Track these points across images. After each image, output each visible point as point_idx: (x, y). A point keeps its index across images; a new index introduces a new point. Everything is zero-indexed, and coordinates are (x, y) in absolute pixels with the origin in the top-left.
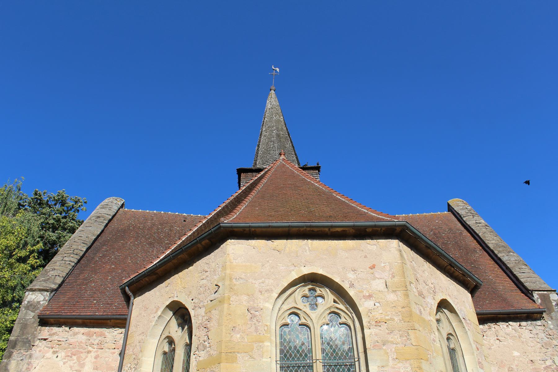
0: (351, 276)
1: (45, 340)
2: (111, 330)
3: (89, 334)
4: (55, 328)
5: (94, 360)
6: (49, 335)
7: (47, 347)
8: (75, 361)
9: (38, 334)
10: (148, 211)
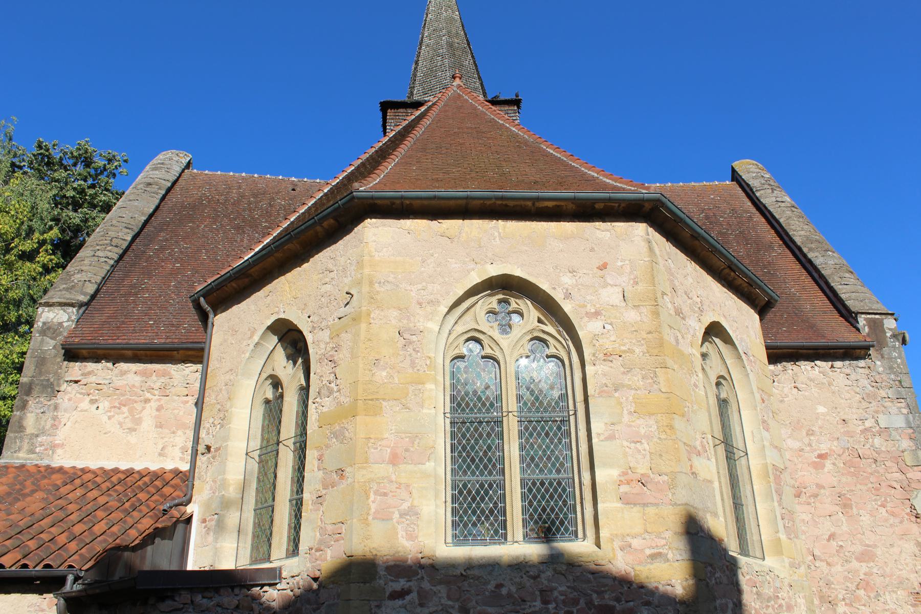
0: (567, 280)
1: (76, 382)
2: (180, 366)
3: (145, 373)
4: (90, 364)
5: (155, 413)
6: (82, 375)
7: (81, 393)
8: (127, 414)
9: (63, 372)
10: (231, 174)
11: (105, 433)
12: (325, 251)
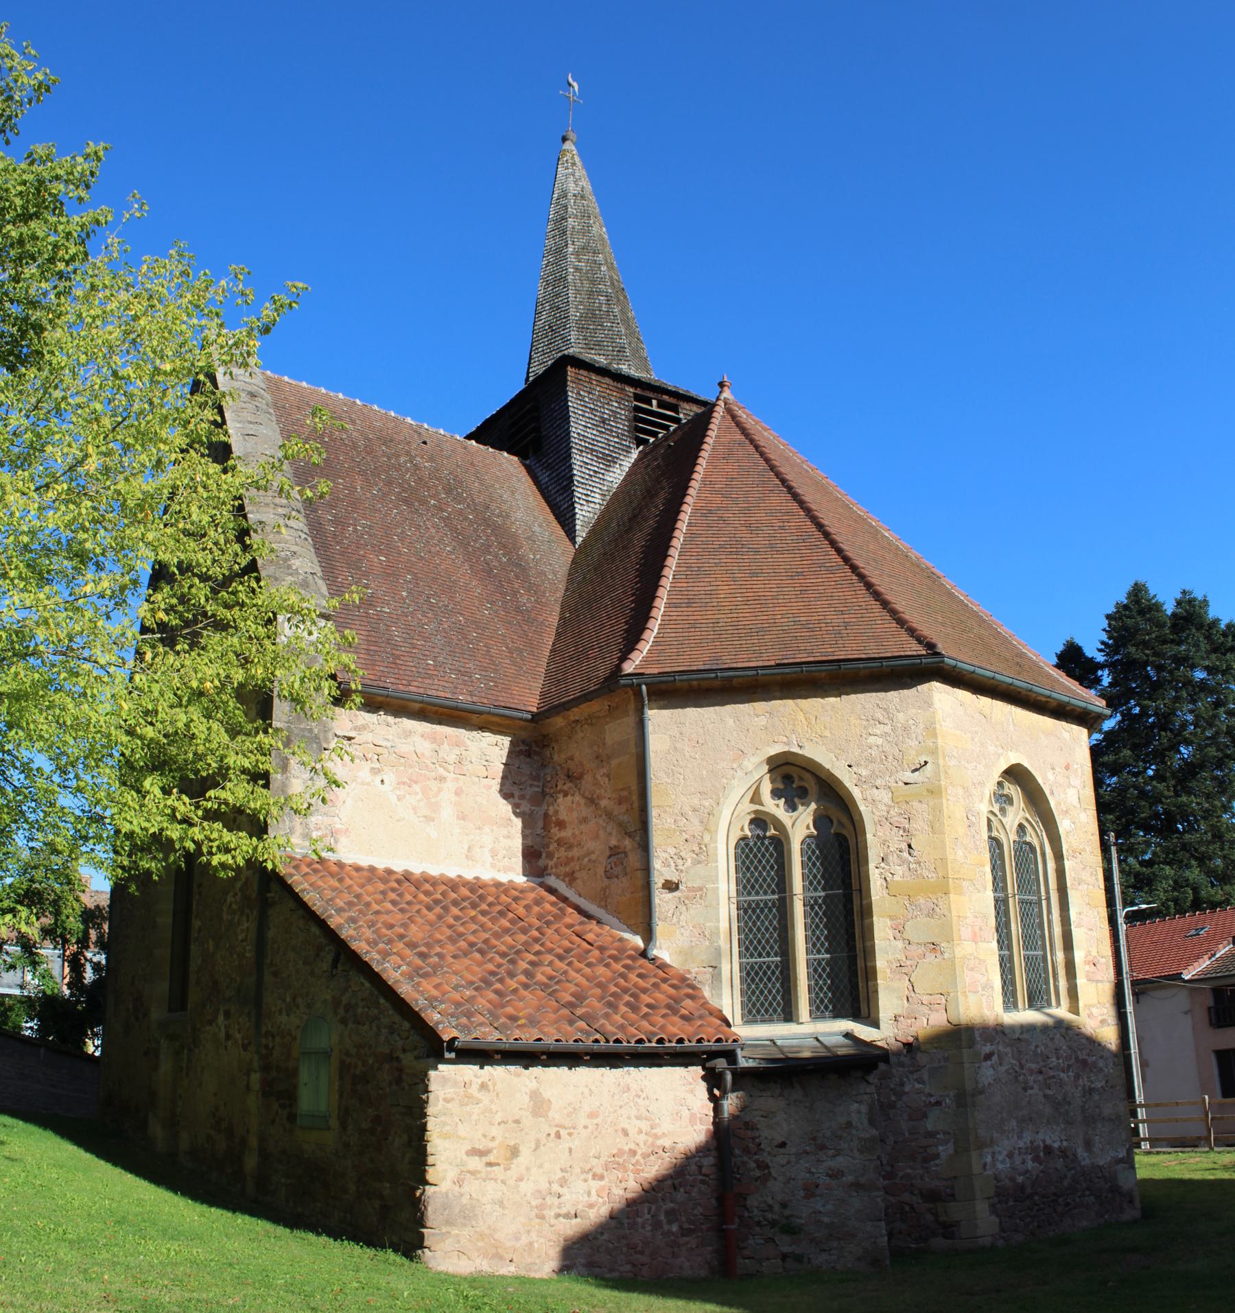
2: (476, 734)
3: (435, 738)
5: (454, 799)
6: (355, 729)
8: (419, 796)
11: (398, 821)
12: (868, 694)
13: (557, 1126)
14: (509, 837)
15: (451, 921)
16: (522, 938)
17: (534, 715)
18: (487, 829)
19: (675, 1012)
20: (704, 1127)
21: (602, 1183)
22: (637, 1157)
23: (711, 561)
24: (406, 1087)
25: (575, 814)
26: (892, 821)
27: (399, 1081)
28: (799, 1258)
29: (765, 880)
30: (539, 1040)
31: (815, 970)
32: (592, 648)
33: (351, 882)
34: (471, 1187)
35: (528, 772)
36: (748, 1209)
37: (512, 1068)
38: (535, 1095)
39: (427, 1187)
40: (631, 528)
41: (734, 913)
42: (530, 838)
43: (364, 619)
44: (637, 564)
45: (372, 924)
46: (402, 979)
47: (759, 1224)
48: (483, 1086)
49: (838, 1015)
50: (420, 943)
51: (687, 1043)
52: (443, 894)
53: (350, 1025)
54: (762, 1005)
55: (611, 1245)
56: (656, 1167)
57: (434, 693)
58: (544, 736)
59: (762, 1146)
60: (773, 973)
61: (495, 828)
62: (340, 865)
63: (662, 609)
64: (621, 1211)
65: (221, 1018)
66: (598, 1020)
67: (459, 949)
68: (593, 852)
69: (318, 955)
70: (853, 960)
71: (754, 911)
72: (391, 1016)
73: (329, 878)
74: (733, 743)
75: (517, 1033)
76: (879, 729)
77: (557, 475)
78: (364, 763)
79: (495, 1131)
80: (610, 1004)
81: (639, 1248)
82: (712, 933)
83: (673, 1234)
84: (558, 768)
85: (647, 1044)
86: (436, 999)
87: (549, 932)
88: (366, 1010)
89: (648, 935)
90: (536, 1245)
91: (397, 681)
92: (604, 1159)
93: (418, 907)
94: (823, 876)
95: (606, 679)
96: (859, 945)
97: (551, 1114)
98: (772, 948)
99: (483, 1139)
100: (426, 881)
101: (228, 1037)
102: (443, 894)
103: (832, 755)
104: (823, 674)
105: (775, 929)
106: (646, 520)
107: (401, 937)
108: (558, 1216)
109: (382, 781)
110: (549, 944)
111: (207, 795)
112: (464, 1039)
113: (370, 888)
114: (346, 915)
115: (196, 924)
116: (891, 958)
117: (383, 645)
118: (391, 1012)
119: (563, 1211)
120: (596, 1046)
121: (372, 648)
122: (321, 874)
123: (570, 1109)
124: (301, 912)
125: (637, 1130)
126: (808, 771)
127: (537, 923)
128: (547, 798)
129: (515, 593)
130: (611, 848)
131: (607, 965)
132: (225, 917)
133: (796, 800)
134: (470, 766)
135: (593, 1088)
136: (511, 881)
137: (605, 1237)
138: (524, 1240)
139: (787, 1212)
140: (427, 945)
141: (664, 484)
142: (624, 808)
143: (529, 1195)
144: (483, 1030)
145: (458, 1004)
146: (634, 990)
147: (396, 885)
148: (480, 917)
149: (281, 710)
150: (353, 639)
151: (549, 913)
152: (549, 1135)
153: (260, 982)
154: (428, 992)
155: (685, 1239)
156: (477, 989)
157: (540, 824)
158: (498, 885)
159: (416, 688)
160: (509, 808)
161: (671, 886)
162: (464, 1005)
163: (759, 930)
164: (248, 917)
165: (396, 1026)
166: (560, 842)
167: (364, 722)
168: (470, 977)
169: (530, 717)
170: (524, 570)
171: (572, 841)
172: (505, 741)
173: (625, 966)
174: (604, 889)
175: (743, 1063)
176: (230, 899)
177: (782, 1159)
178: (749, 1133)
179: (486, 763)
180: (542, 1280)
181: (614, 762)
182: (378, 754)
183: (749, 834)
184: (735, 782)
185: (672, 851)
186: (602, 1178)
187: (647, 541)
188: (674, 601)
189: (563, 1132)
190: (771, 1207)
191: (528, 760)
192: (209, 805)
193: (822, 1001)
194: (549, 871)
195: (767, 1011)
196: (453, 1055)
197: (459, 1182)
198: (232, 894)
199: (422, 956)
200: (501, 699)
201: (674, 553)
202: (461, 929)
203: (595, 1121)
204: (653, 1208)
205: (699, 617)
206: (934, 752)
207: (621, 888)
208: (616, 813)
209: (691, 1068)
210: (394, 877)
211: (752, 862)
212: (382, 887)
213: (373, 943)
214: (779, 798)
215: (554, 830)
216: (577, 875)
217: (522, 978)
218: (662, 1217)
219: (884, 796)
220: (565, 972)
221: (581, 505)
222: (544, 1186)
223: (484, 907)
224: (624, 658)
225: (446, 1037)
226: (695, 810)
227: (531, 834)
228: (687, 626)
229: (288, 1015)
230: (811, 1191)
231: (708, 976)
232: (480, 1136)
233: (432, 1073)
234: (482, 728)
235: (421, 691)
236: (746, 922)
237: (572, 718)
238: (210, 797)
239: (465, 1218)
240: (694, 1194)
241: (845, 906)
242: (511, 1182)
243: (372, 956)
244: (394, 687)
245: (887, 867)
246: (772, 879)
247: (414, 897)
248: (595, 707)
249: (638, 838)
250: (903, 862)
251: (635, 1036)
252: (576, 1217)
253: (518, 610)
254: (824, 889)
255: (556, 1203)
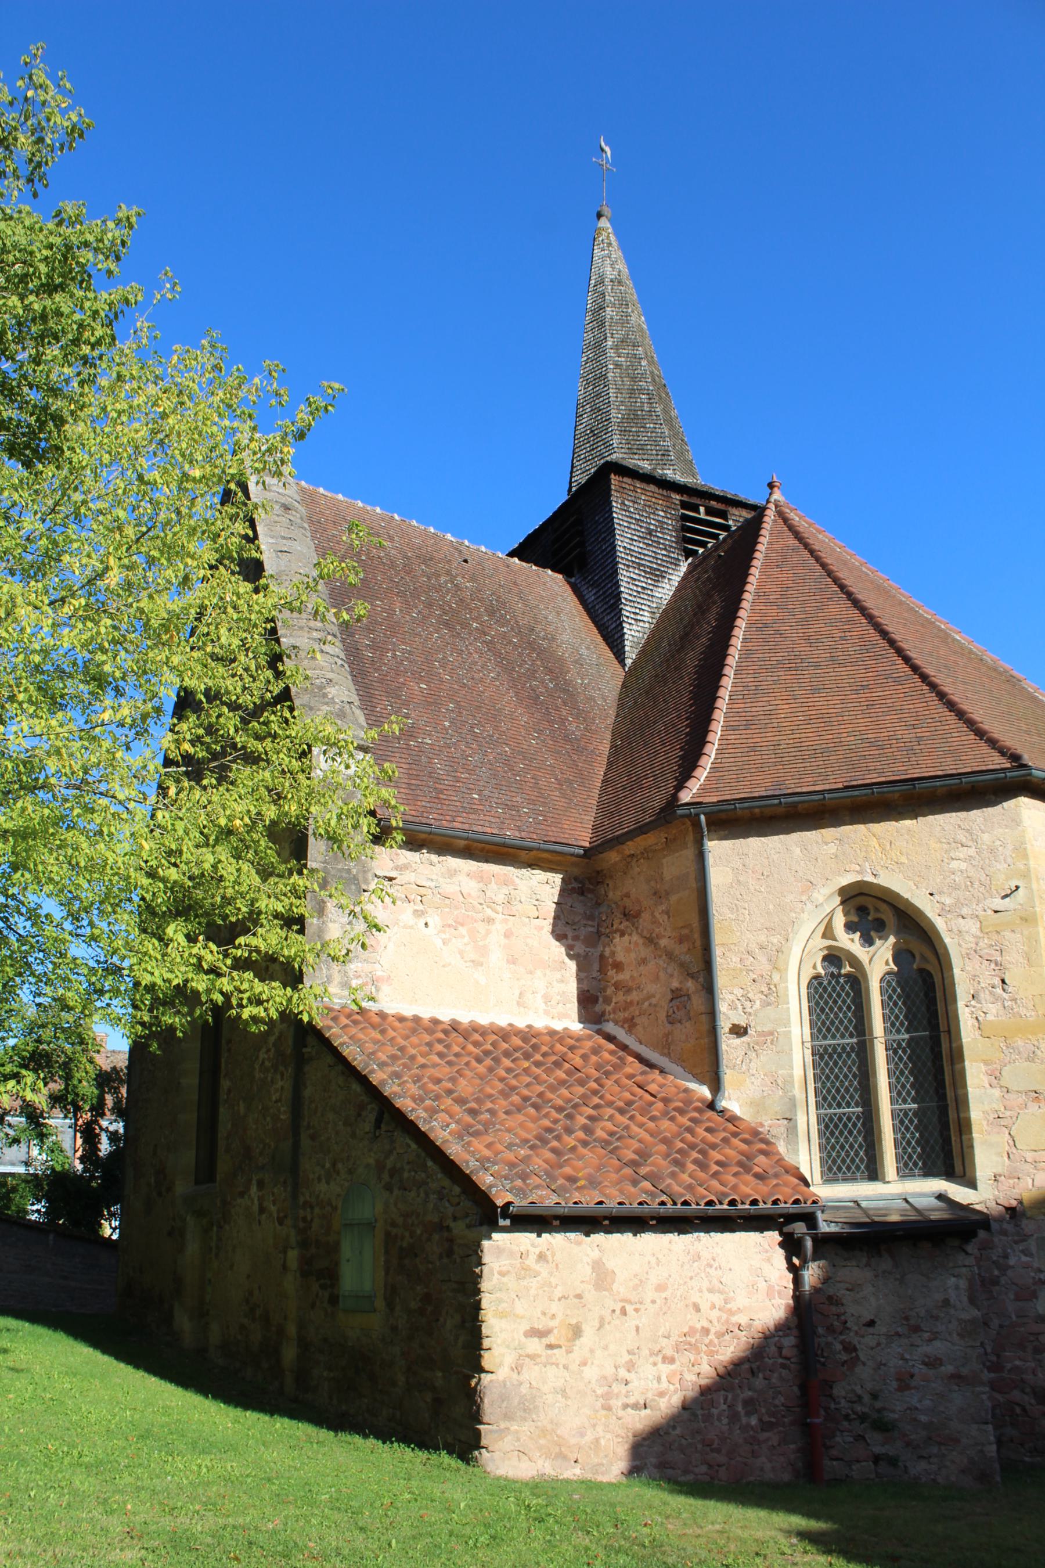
3: (482, 877)
5: (503, 941)
6: (397, 868)
8: (466, 940)
11: (444, 966)
13: (622, 1301)
14: (562, 981)
15: (503, 1073)
16: (581, 1090)
17: (587, 851)
18: (539, 973)
19: (747, 1169)
20: (783, 1302)
21: (673, 1367)
22: (710, 1337)
23: (769, 678)
24: (458, 1260)
25: (633, 955)
26: (981, 953)
27: (450, 1253)
28: (893, 1461)
29: (841, 1022)
30: (601, 1203)
31: (902, 1122)
32: (646, 777)
33: (394, 1034)
34: (531, 1373)
35: (582, 911)
36: (834, 1400)
37: (572, 1235)
38: (598, 1266)
39: (483, 1375)
40: (682, 647)
41: (809, 1059)
42: (585, 982)
43: (405, 751)
44: (691, 685)
45: (417, 1079)
46: (451, 1139)
47: (847, 1417)
48: (541, 1257)
49: (928, 1173)
50: (470, 1099)
51: (761, 1205)
52: (494, 1044)
53: (396, 1192)
54: (844, 1161)
55: (683, 1441)
56: (732, 1349)
57: (480, 829)
58: (598, 872)
59: (848, 1325)
60: (854, 1125)
61: (548, 972)
62: (382, 1015)
63: (719, 733)
64: (695, 1400)
65: (254, 1189)
66: (664, 1180)
67: (512, 1104)
68: (653, 996)
69: (359, 1115)
70: (943, 1110)
71: (831, 1057)
72: (440, 1180)
73: (371, 1030)
74: (800, 874)
75: (577, 1196)
76: (962, 853)
77: (604, 593)
78: (406, 904)
79: (555, 1307)
80: (676, 1162)
81: (715, 1446)
82: (785, 1082)
83: (752, 1428)
84: (614, 906)
85: (718, 1207)
86: (488, 1159)
87: (609, 1083)
88: (413, 1173)
89: (716, 1085)
90: (603, 1442)
91: (441, 817)
92: (674, 1338)
93: (466, 1059)
94: (906, 1017)
95: (662, 810)
96: (950, 1094)
97: (615, 1287)
98: (852, 1097)
99: (542, 1318)
100: (476, 1031)
101: (262, 1210)
102: (493, 1044)
103: (911, 883)
104: (897, 795)
105: (855, 1076)
106: (698, 638)
107: (449, 1092)
108: (626, 1406)
109: (426, 924)
110: (608, 1097)
111: (237, 942)
112: (519, 1203)
113: (414, 1040)
114: (390, 1069)
115: (225, 1084)
116: (987, 1108)
117: (424, 778)
118: (440, 1176)
119: (631, 1400)
120: (662, 1210)
121: (413, 782)
122: (362, 1026)
123: (636, 1281)
124: (340, 1067)
125: (709, 1304)
126: (884, 901)
127: (596, 1074)
128: (603, 938)
129: (563, 720)
130: (672, 991)
131: (672, 1119)
132: (258, 1075)
133: (873, 933)
134: (519, 906)
135: (660, 1257)
136: (566, 1029)
137: (678, 1431)
138: (589, 1437)
139: (878, 1405)
140: (478, 1100)
141: (716, 598)
142: (684, 947)
143: (593, 1381)
144: (540, 1193)
145: (512, 1165)
146: (702, 1146)
147: (442, 1036)
148: (534, 1068)
149: (317, 851)
150: (393, 772)
151: (608, 1062)
152: (614, 1311)
153: (296, 1146)
154: (479, 1152)
155: (766, 1435)
156: (532, 1148)
157: (596, 966)
158: (552, 1033)
159: (460, 824)
160: (563, 950)
161: (739, 1031)
162: (519, 1165)
163: (837, 1077)
164: (282, 1075)
165: (445, 1191)
166: (617, 986)
167: (406, 861)
168: (525, 1135)
169: (582, 852)
170: (572, 695)
171: (630, 984)
172: (557, 879)
173: (691, 1120)
174: (667, 1035)
175: (824, 1228)
176: (262, 1055)
177: (870, 1341)
178: (833, 1309)
179: (536, 903)
180: (610, 1484)
181: (674, 898)
182: (421, 894)
183: (823, 972)
184: (805, 916)
185: (739, 992)
186: (672, 1361)
187: (700, 660)
188: (732, 723)
189: (629, 1308)
190: (860, 1397)
191: (581, 898)
192: (239, 953)
193: (910, 1157)
194: (607, 1017)
195: (849, 1168)
196: (508, 1222)
197: (517, 1368)
198: (264, 1050)
199: (473, 1112)
200: (550, 833)
201: (729, 671)
202: (514, 1082)
203: (664, 1295)
204: (730, 1396)
205: (758, 740)
206: (1026, 875)
207: (685, 1033)
208: (677, 952)
209: (766, 1233)
210: (441, 1027)
211: (826, 1003)
212: (427, 1038)
213: (418, 1100)
214: (854, 932)
215: (611, 973)
216: (637, 1020)
217: (581, 1134)
218: (740, 1408)
219: (971, 926)
220: (627, 1128)
221: (630, 624)
222: (610, 1371)
223: (538, 1057)
224: (680, 786)
225: (500, 1202)
226: (762, 948)
227: (587, 977)
228: (747, 750)
229: (328, 1183)
230: (905, 1381)
231: (783, 1129)
232: (540, 1315)
233: (485, 1243)
234: (531, 865)
235: (466, 827)
236: (823, 1069)
237: (627, 852)
238: (240, 944)
239: (525, 1410)
240: (774, 1380)
241: (932, 1049)
242: (574, 1367)
243: (418, 1114)
244: (437, 823)
245: (979, 1005)
246: (850, 1021)
247: (463, 1048)
248: (650, 839)
249: (701, 979)
250: (996, 999)
251: (704, 1197)
252: (645, 1407)
253: (567, 739)
254: (908, 1031)
255: (624, 1392)
